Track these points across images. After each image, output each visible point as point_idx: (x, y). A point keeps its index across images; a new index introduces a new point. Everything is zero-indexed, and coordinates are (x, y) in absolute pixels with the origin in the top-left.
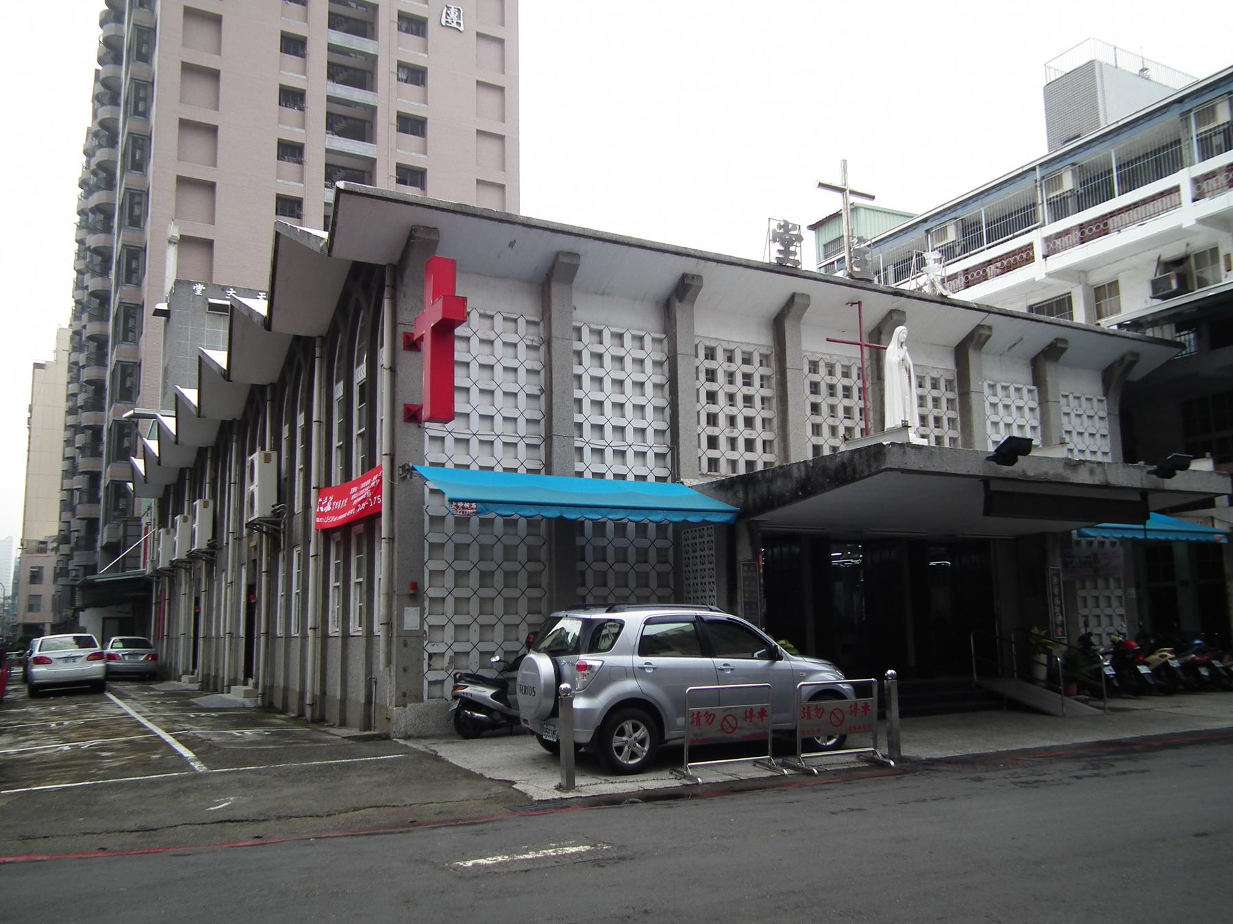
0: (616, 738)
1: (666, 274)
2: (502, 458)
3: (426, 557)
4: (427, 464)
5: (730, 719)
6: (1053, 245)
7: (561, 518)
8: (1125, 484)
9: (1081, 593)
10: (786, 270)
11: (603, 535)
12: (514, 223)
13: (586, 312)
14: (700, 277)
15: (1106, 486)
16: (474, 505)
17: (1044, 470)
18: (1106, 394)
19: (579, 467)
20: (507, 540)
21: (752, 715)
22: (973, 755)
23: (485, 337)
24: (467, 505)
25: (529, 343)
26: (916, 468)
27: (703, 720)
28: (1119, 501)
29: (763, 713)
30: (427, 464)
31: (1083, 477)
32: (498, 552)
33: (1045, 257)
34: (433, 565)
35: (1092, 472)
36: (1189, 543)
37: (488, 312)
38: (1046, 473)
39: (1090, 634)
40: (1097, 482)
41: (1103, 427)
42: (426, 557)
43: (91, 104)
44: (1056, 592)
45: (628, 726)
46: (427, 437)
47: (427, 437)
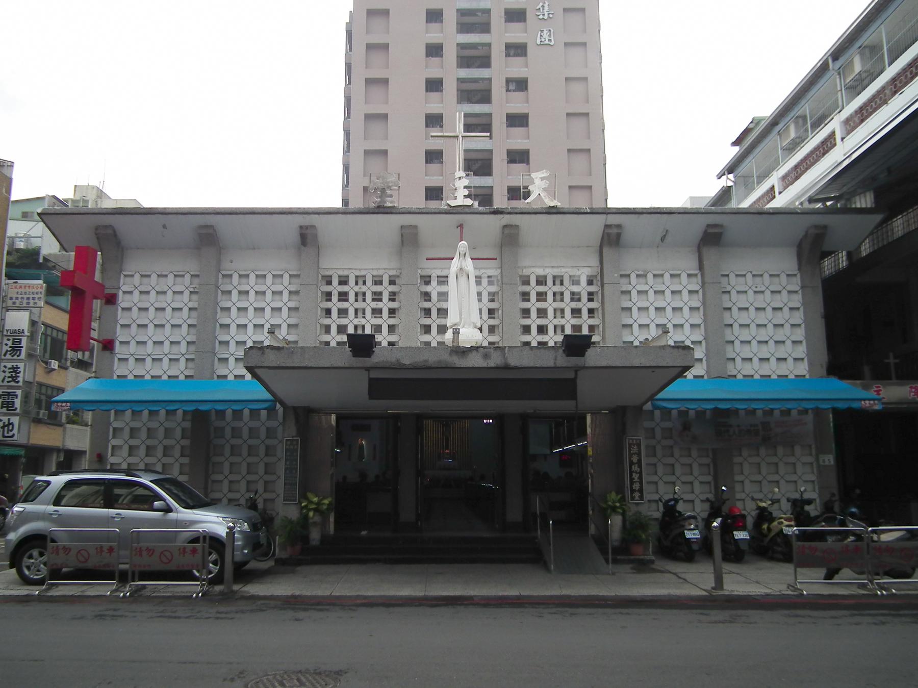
0: (25, 559)
1: (290, 229)
2: (164, 369)
3: (111, 437)
4: (115, 377)
5: (83, 552)
6: (851, 124)
7: (197, 410)
8: (532, 365)
9: (737, 460)
10: (386, 210)
11: (241, 419)
12: (154, 214)
13: (236, 263)
14: (313, 227)
15: (507, 367)
16: (68, 404)
17: (425, 358)
18: (799, 269)
19: (222, 371)
20: (168, 425)
21: (102, 551)
22: (346, 596)
23: (160, 290)
24: (64, 404)
25: (192, 290)
26: (274, 364)
27: (144, 553)
28: (549, 380)
29: (111, 550)
30: (115, 377)
31: (475, 361)
32: (161, 433)
33: (843, 139)
34: (114, 442)
35: (486, 356)
36: (835, 411)
37: (164, 273)
38: (426, 361)
39: (676, 501)
40: (492, 365)
41: (797, 301)
42: (111, 437)
43: (14, 177)
44: (635, 459)
45: (35, 553)
46: (116, 360)
47: (116, 360)
